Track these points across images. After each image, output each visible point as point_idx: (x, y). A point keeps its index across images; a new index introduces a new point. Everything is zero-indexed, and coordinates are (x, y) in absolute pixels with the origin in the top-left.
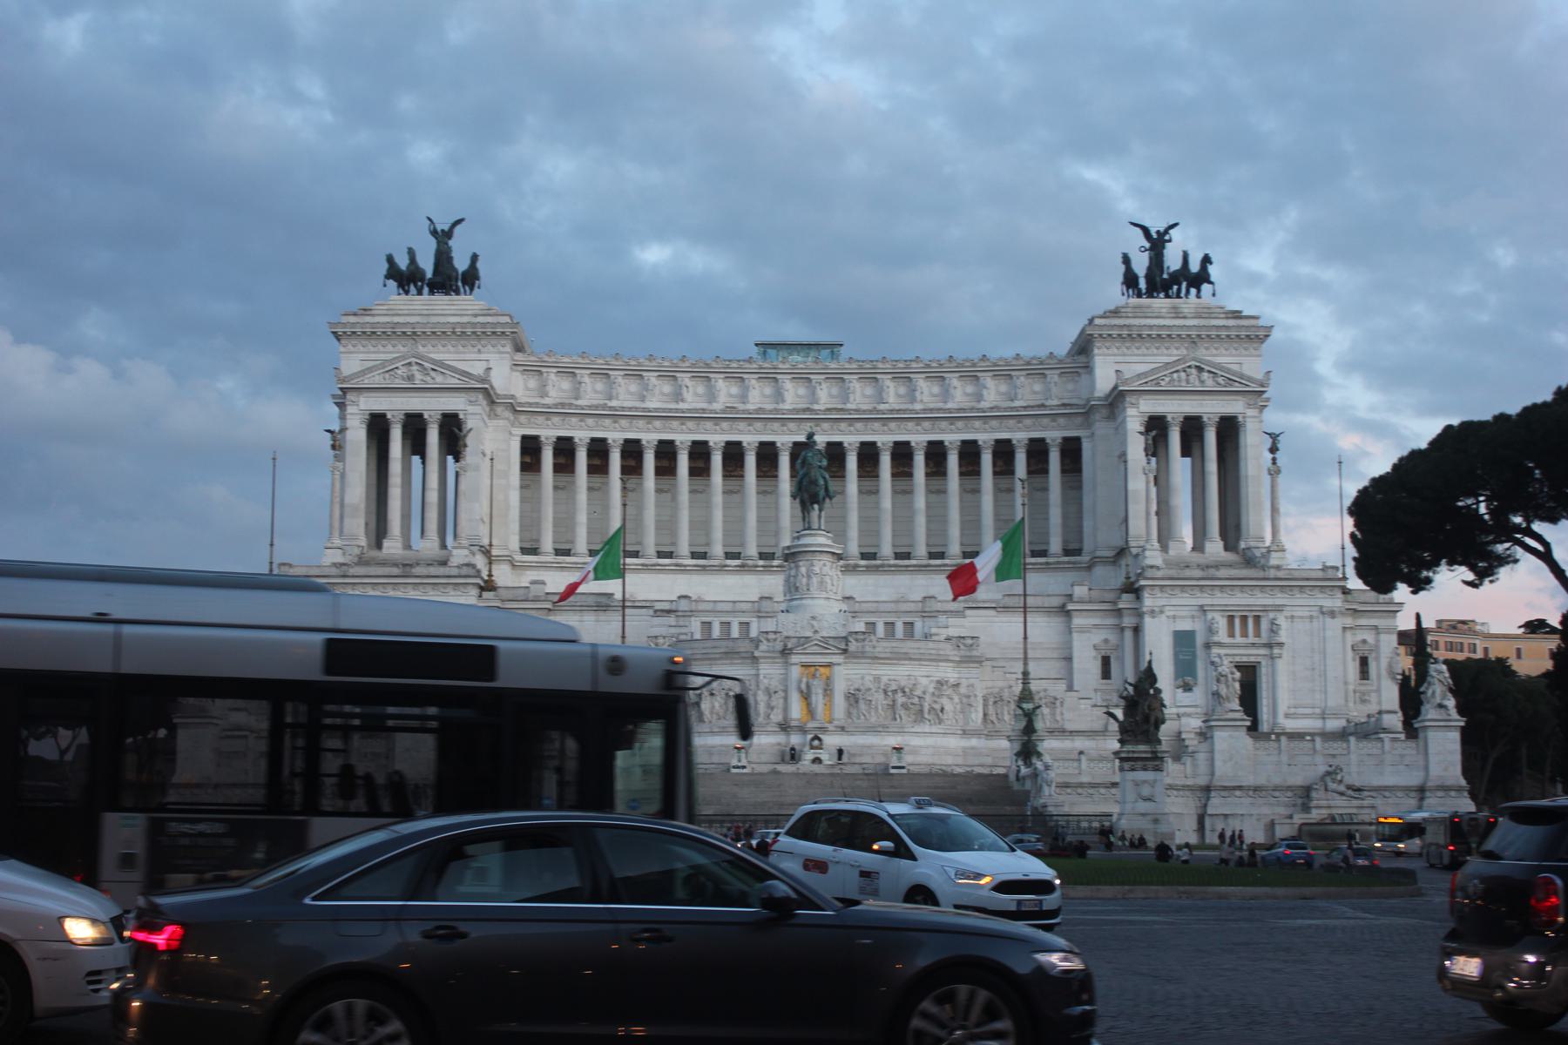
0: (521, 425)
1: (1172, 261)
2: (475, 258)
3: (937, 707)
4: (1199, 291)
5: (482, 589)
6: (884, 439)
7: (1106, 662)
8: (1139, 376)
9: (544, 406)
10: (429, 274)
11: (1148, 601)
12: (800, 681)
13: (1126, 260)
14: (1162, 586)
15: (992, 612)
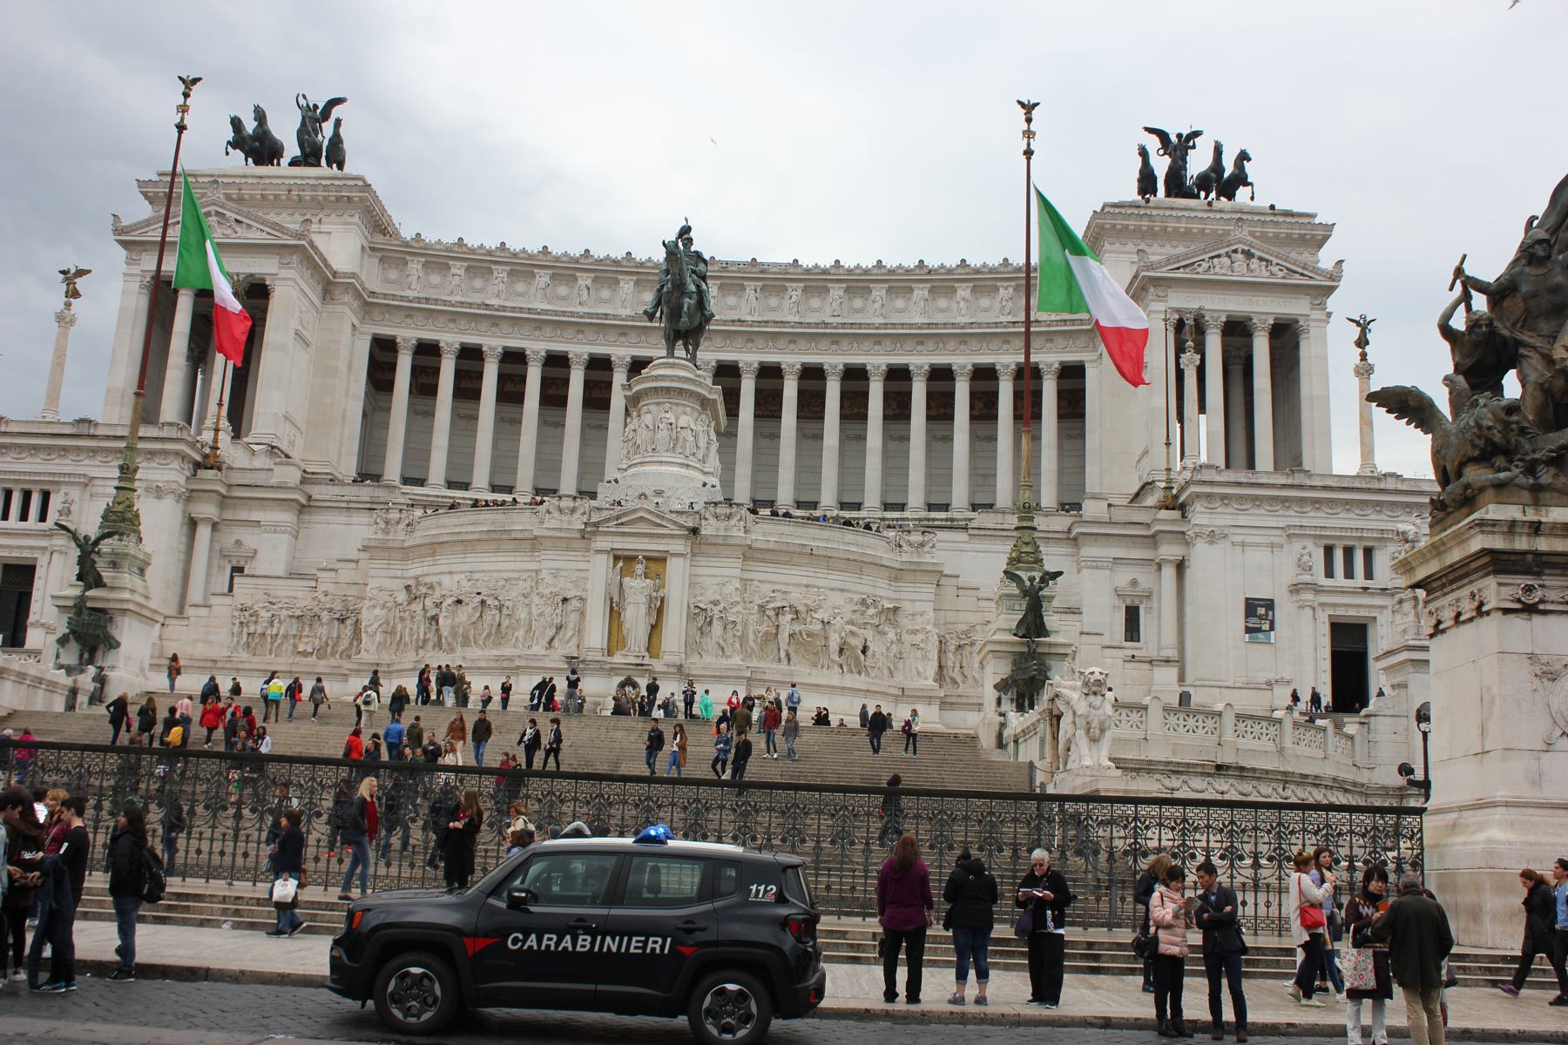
0: (374, 322)
1: (1198, 162)
2: (338, 122)
3: (857, 643)
4: (1231, 197)
5: (198, 466)
6: (834, 360)
7: (1132, 616)
8: (1168, 261)
9: (402, 298)
10: (292, 149)
11: (1200, 516)
12: (608, 585)
13: (1143, 153)
14: (1224, 497)
15: (962, 536)
